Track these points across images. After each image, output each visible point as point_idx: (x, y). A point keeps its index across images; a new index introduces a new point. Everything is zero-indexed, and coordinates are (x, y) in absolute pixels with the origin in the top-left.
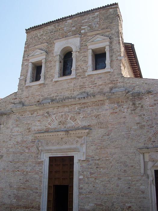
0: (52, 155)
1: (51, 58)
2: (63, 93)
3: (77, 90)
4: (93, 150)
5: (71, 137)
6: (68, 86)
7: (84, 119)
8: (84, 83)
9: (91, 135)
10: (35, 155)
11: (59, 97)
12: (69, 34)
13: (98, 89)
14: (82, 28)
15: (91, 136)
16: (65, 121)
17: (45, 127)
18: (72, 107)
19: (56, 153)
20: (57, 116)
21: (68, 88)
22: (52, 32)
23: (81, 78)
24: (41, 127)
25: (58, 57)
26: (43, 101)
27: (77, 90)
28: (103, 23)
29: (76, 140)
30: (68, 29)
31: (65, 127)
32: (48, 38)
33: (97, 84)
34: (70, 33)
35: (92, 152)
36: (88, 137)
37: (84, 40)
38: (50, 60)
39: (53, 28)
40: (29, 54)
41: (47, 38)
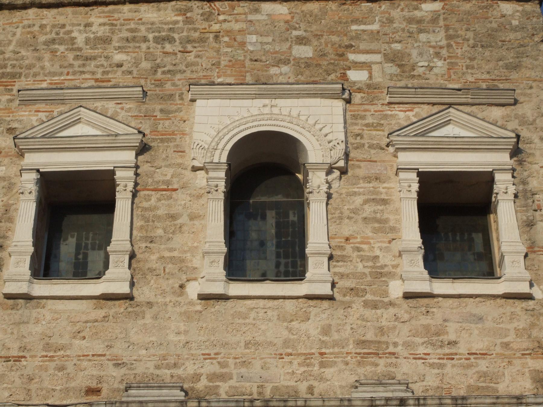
1: (170, 172)
2: (257, 364)
3: (347, 364)
6: (285, 333)
8: (381, 330)
11: (232, 383)
12: (274, 70)
13: (470, 372)
14: (352, 57)
21: (286, 343)
22: (171, 40)
23: (366, 304)
25: (222, 174)
26: (132, 392)
27: (347, 364)
28: (472, 59)
30: (267, 47)
32: (145, 65)
33: (462, 349)
34: (285, 69)
37: (370, 120)
38: (164, 182)
39: (176, 22)
40: (15, 125)
41: (137, 64)
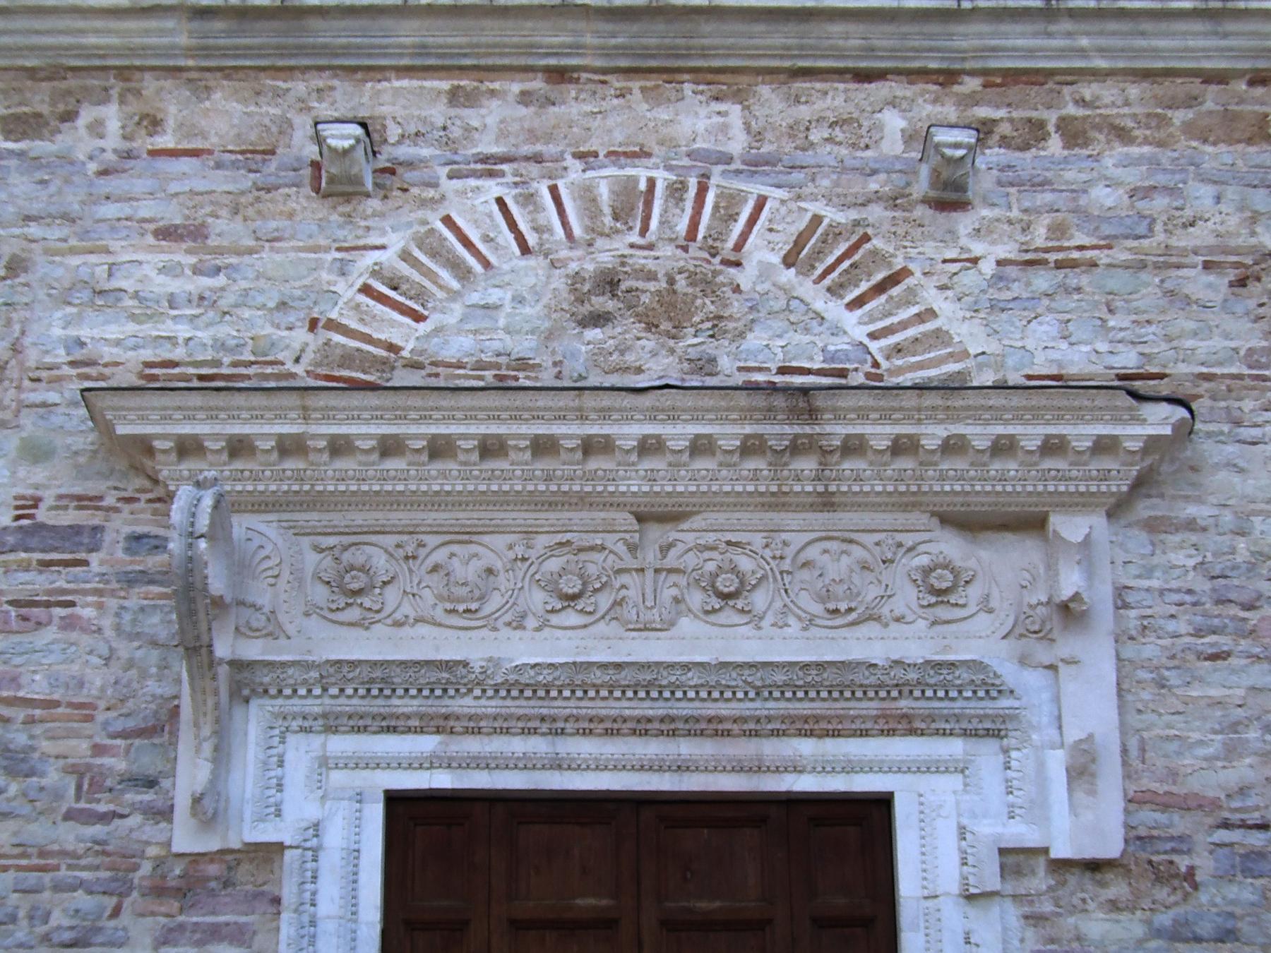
0: (449, 764)
4: (1235, 727)
5: (827, 502)
7: (1042, 281)
9: (1192, 510)
10: (98, 750)
15: (1191, 525)
16: (693, 279)
17: (301, 336)
18: (804, 112)
19: (538, 745)
20: (529, 199)
24: (226, 331)
29: (924, 560)
31: (705, 365)
35: (1231, 752)
36: (1143, 536)
